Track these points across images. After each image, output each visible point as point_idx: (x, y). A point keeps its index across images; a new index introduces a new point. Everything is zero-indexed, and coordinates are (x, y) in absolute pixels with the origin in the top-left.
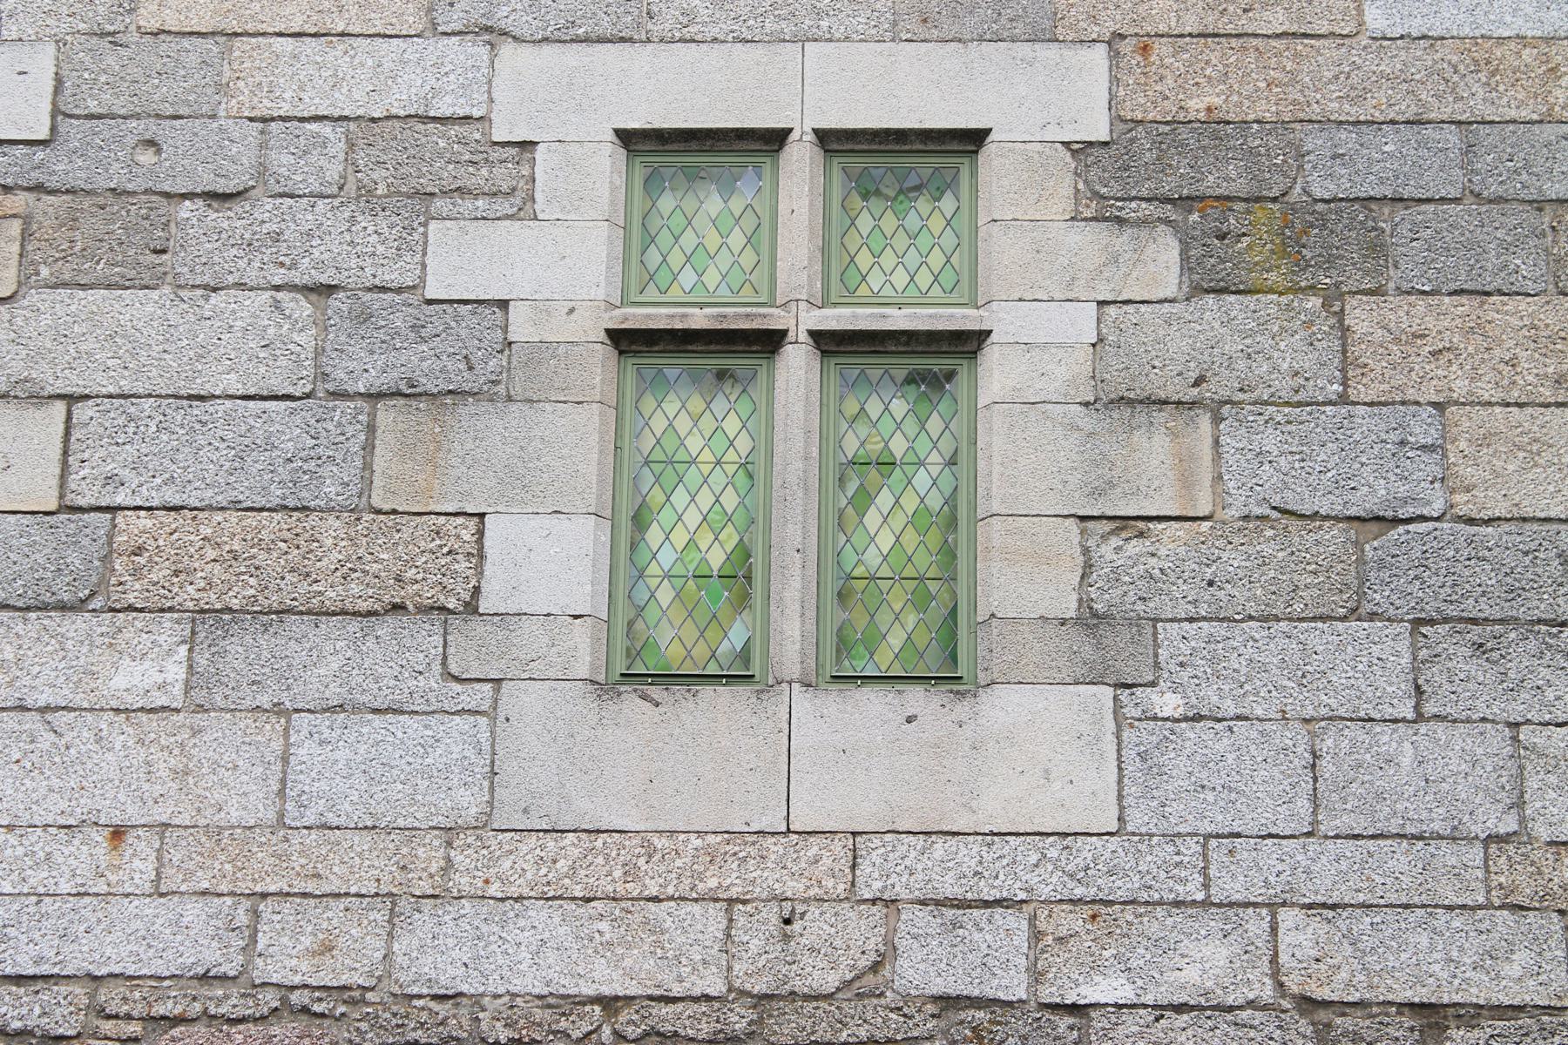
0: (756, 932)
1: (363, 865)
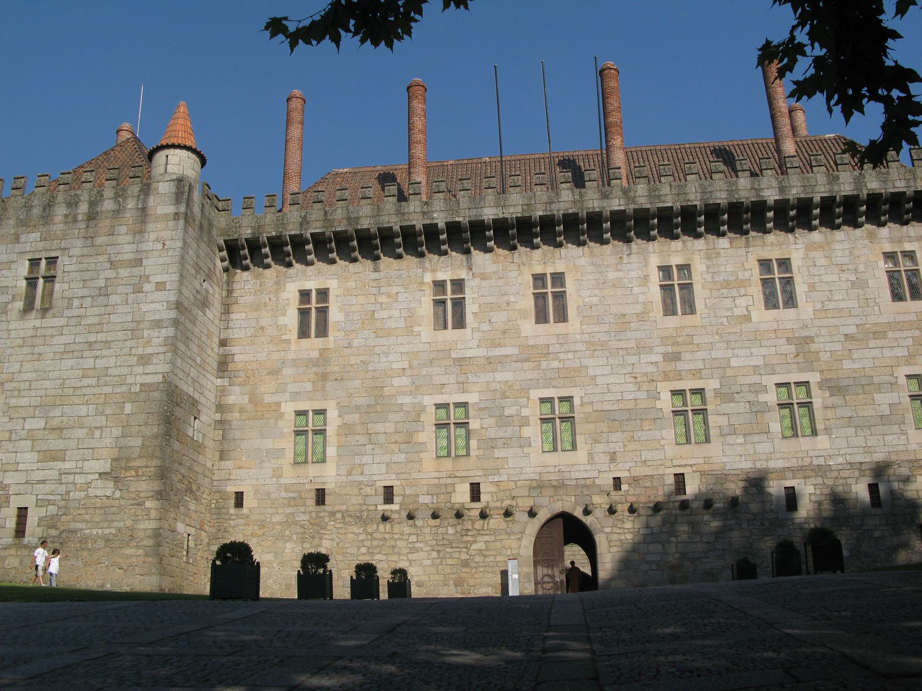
0: (800, 460)
1: (764, 457)
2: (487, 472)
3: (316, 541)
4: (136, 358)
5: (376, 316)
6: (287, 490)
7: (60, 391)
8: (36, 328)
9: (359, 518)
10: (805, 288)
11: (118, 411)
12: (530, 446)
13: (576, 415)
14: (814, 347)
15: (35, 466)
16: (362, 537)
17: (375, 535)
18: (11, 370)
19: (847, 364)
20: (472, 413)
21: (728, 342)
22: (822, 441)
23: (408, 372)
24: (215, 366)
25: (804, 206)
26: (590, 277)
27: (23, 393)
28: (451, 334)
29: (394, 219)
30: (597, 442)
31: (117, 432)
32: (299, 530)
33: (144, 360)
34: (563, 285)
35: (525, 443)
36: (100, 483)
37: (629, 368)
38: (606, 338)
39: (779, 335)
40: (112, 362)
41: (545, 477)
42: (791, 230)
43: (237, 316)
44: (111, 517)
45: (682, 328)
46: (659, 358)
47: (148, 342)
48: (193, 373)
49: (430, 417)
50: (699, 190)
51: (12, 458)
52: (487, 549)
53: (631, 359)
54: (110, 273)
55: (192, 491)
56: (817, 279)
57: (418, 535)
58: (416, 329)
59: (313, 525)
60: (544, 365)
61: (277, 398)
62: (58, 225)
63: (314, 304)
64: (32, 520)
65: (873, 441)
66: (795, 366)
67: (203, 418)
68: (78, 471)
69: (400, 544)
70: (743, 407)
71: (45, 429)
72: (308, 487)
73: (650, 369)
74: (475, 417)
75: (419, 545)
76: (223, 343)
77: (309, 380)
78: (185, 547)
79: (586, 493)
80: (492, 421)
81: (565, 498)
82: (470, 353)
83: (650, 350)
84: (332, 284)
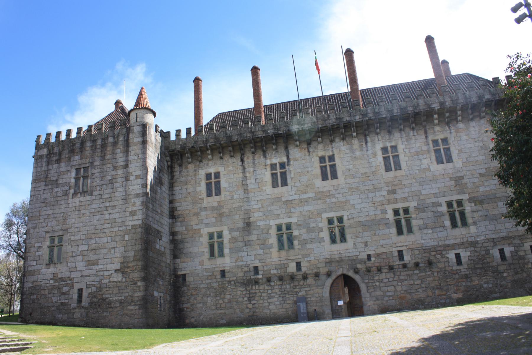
0: (462, 240)
1: (443, 239)
2: (304, 256)
3: (222, 296)
4: (128, 213)
5: (244, 183)
6: (207, 272)
7: (94, 231)
8: (80, 202)
9: (244, 283)
10: (457, 152)
11: (122, 239)
12: (324, 241)
13: (346, 225)
14: (464, 181)
15: (84, 268)
16: (244, 293)
17: (251, 291)
18: (70, 223)
19: (481, 189)
20: (293, 227)
21: (420, 182)
22: (473, 229)
23: (261, 210)
24: (168, 213)
25: (453, 111)
26: (347, 155)
27: (76, 233)
28: (281, 190)
29: (249, 135)
30: (357, 237)
31: (122, 249)
32: (214, 291)
33: (133, 213)
34: (334, 161)
35: (322, 240)
36: (115, 275)
37: (371, 200)
38: (358, 185)
39: (445, 177)
40: (117, 215)
41: (333, 257)
42: (448, 124)
43: (177, 188)
44: (121, 291)
45: (396, 177)
46: (385, 193)
47: (134, 205)
48: (157, 217)
49: (273, 231)
50: (398, 108)
51: (74, 265)
52: (306, 295)
53: (371, 195)
54: (114, 173)
55: (160, 275)
56: (462, 147)
57: (272, 290)
58: (264, 188)
59: (220, 288)
60: (328, 201)
61: (199, 227)
62: (88, 151)
63: (213, 180)
64: (85, 294)
65: (499, 227)
66: (455, 192)
67: (163, 239)
68: (105, 269)
69: (263, 294)
70: (430, 214)
71: (88, 250)
72: (216, 269)
73: (382, 199)
74: (296, 229)
75: (272, 295)
76: (171, 202)
77: (213, 217)
78: (159, 303)
79: (354, 263)
80: (303, 231)
81: (344, 266)
82: (291, 198)
83: (380, 189)
84: (221, 169)
